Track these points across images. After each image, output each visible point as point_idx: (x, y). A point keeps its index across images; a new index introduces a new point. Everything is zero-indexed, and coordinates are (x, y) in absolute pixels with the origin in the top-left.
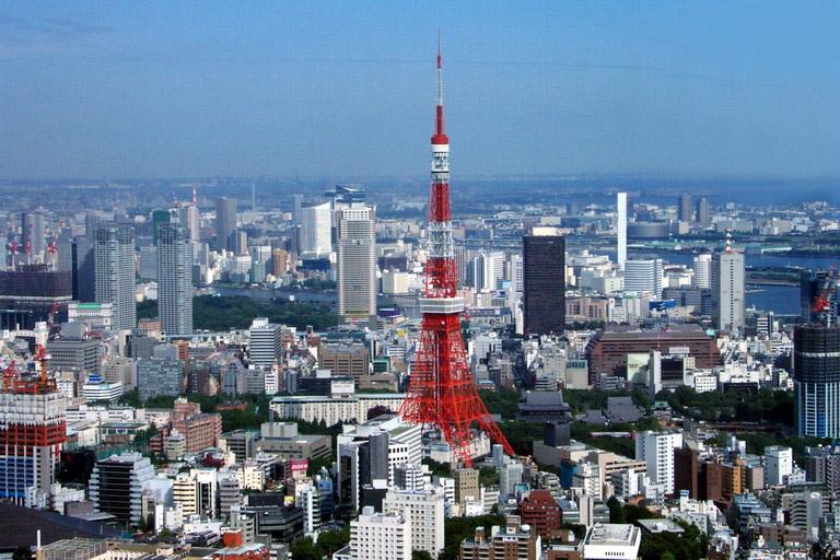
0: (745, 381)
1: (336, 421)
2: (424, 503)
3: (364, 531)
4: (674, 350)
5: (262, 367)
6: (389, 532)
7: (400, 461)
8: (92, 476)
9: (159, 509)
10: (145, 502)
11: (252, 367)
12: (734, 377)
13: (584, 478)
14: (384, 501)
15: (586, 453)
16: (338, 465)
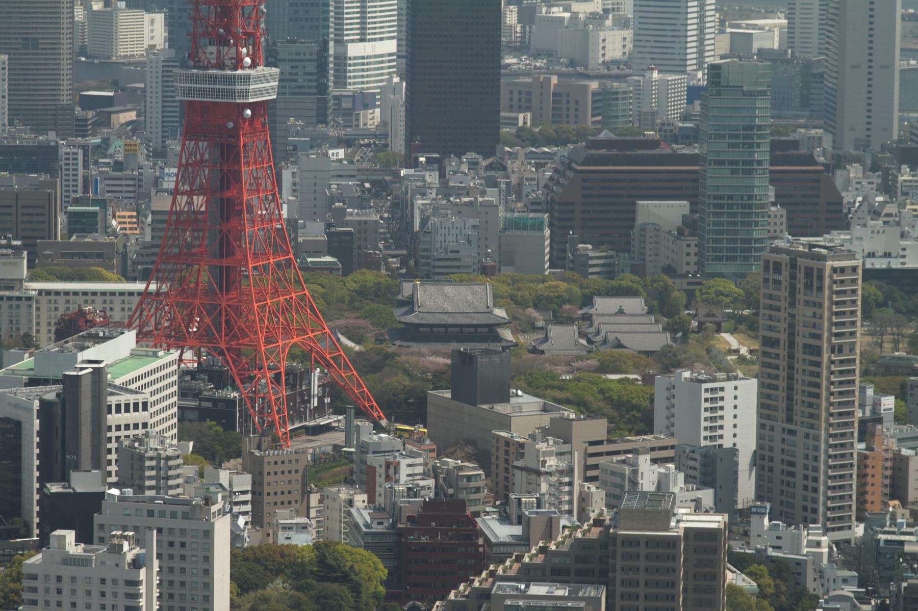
0: (895, 264)
3: (53, 585)
6: (108, 588)
7: (131, 432)
13: (539, 473)
14: (97, 518)
15: (545, 420)
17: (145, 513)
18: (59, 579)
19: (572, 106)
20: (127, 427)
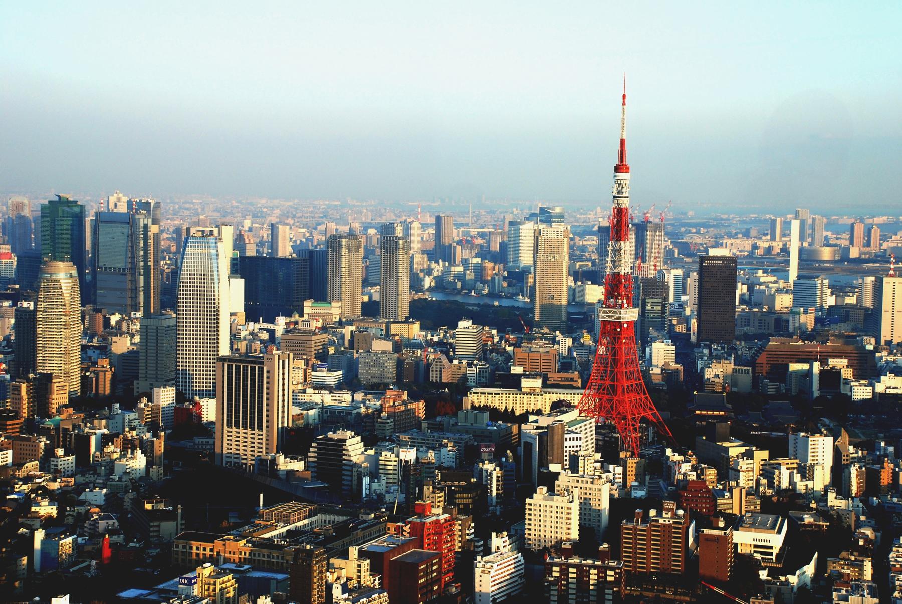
1: (524, 411)
2: (591, 486)
3: (537, 508)
4: (833, 362)
5: (464, 362)
8: (311, 449)
9: (366, 480)
10: (355, 474)
11: (455, 362)
12: (888, 388)
13: (739, 471)
15: (743, 450)
16: (521, 449)
17: (576, 481)
18: (540, 506)
19: (767, 324)
20: (573, 447)
